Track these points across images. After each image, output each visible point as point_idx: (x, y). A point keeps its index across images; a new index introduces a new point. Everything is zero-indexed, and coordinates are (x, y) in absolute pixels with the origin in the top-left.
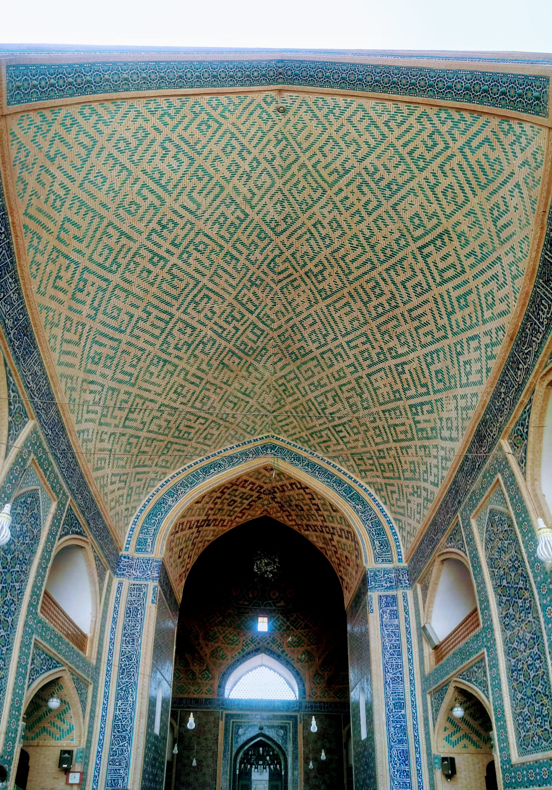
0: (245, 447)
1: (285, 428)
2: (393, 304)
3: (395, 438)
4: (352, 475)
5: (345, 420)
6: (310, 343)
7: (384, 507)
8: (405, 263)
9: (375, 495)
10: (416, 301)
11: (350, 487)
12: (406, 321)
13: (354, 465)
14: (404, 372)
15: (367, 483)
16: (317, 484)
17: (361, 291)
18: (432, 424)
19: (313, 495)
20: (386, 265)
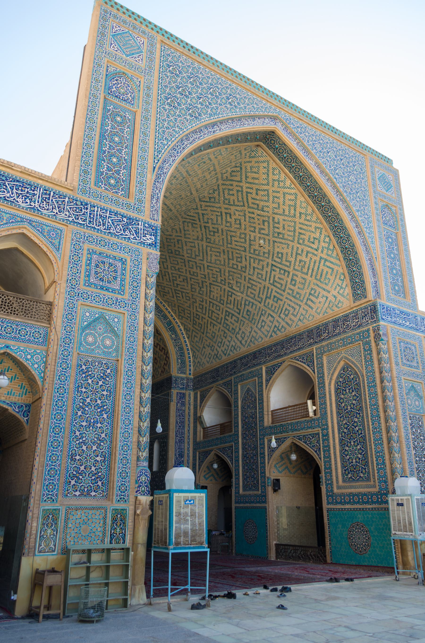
2: (244, 269)
3: (210, 316)
4: (173, 314)
6: (185, 252)
7: (187, 339)
8: (261, 263)
9: (183, 331)
10: (255, 278)
11: (170, 321)
12: (245, 280)
13: (177, 311)
14: (231, 296)
15: (181, 322)
17: (230, 253)
18: (234, 327)
20: (251, 255)
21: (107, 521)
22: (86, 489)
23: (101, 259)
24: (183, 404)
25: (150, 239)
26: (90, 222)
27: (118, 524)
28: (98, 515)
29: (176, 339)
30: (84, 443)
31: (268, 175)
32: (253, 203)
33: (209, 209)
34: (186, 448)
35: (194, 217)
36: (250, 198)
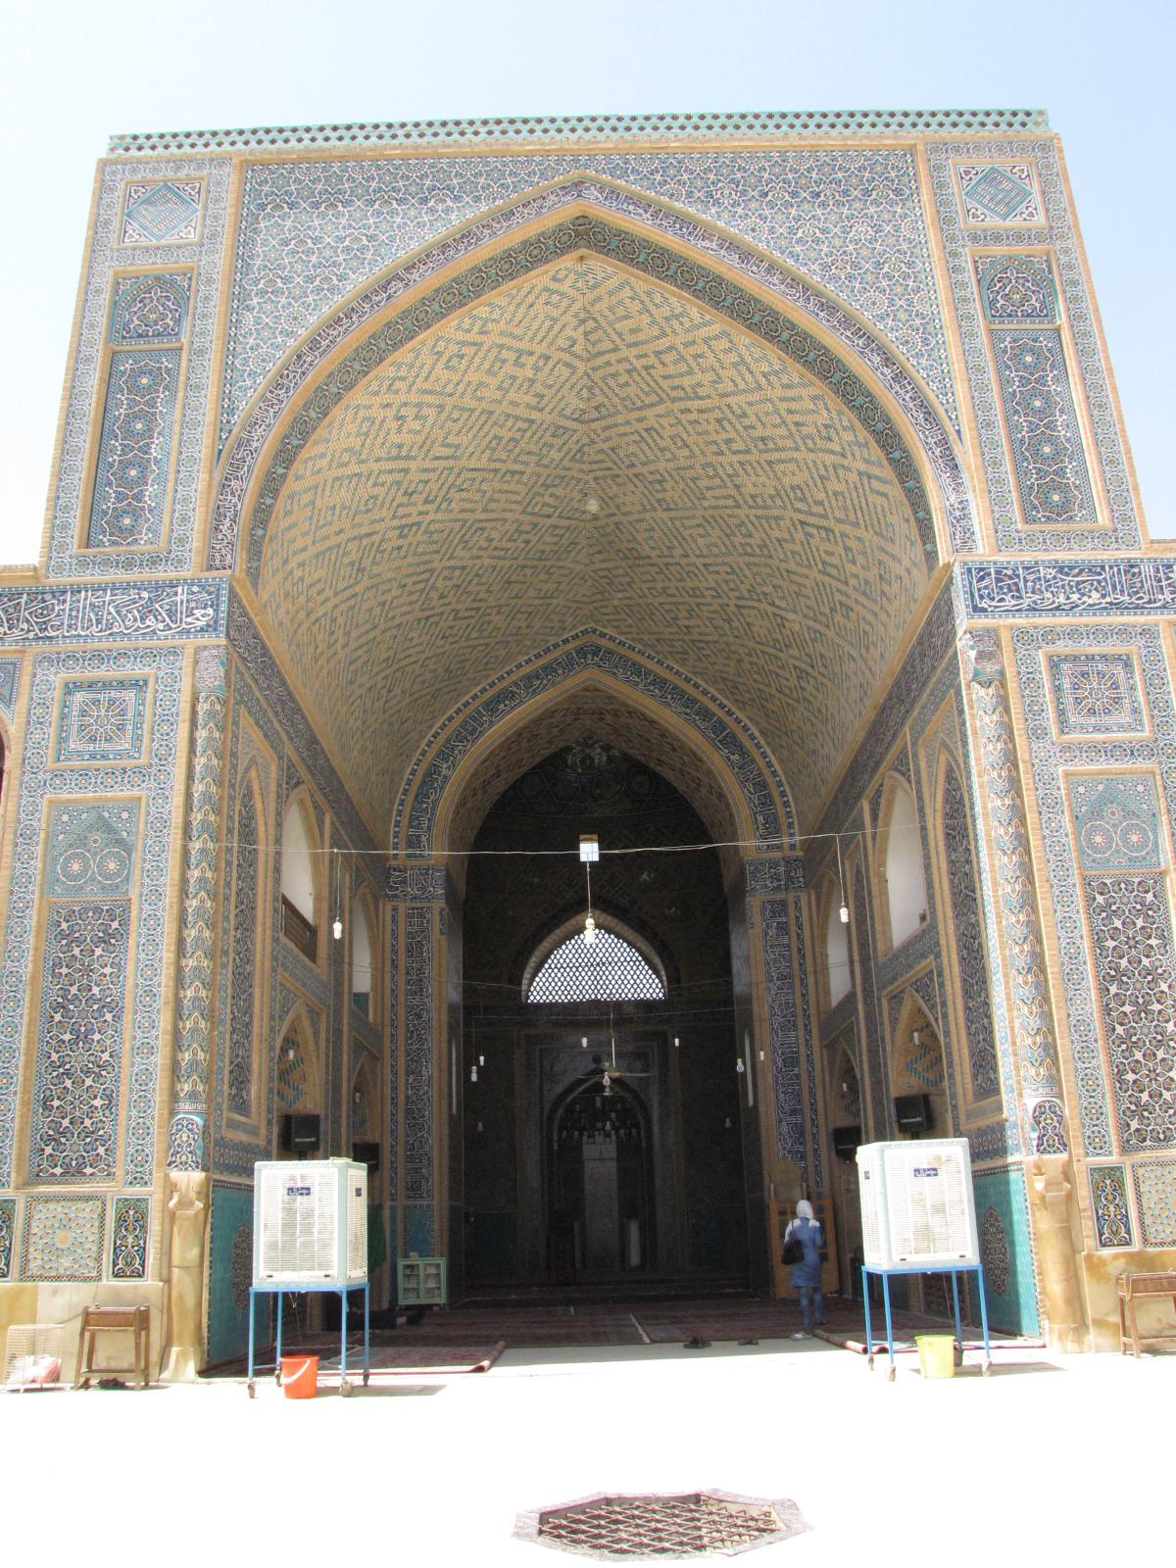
0: (550, 657)
1: (615, 624)
4: (725, 702)
5: (709, 638)
11: (720, 721)
16: (670, 717)
19: (664, 734)
21: (107, 1222)
22: (74, 1163)
23: (91, 696)
24: (783, 929)
25: (202, 617)
26: (70, 626)
27: (131, 1228)
28: (89, 1210)
29: (744, 764)
30: (67, 1073)
31: (648, 311)
32: (674, 388)
33: (613, 432)
34: (802, 1041)
35: (601, 461)
36: (660, 380)
